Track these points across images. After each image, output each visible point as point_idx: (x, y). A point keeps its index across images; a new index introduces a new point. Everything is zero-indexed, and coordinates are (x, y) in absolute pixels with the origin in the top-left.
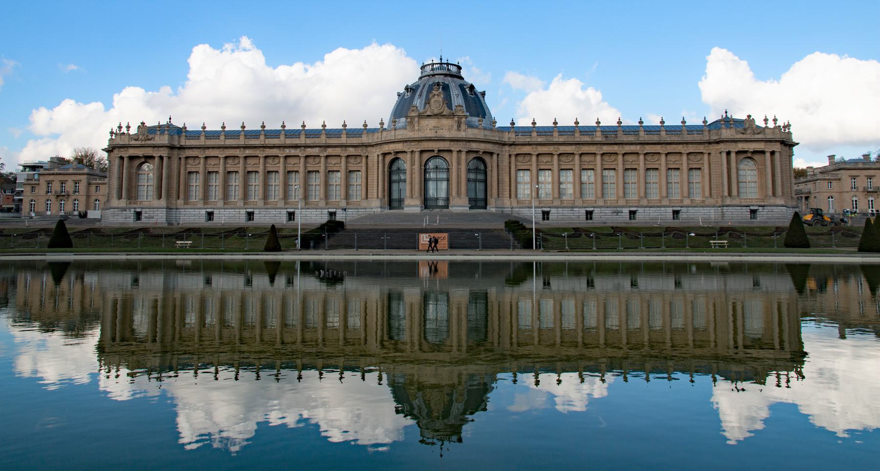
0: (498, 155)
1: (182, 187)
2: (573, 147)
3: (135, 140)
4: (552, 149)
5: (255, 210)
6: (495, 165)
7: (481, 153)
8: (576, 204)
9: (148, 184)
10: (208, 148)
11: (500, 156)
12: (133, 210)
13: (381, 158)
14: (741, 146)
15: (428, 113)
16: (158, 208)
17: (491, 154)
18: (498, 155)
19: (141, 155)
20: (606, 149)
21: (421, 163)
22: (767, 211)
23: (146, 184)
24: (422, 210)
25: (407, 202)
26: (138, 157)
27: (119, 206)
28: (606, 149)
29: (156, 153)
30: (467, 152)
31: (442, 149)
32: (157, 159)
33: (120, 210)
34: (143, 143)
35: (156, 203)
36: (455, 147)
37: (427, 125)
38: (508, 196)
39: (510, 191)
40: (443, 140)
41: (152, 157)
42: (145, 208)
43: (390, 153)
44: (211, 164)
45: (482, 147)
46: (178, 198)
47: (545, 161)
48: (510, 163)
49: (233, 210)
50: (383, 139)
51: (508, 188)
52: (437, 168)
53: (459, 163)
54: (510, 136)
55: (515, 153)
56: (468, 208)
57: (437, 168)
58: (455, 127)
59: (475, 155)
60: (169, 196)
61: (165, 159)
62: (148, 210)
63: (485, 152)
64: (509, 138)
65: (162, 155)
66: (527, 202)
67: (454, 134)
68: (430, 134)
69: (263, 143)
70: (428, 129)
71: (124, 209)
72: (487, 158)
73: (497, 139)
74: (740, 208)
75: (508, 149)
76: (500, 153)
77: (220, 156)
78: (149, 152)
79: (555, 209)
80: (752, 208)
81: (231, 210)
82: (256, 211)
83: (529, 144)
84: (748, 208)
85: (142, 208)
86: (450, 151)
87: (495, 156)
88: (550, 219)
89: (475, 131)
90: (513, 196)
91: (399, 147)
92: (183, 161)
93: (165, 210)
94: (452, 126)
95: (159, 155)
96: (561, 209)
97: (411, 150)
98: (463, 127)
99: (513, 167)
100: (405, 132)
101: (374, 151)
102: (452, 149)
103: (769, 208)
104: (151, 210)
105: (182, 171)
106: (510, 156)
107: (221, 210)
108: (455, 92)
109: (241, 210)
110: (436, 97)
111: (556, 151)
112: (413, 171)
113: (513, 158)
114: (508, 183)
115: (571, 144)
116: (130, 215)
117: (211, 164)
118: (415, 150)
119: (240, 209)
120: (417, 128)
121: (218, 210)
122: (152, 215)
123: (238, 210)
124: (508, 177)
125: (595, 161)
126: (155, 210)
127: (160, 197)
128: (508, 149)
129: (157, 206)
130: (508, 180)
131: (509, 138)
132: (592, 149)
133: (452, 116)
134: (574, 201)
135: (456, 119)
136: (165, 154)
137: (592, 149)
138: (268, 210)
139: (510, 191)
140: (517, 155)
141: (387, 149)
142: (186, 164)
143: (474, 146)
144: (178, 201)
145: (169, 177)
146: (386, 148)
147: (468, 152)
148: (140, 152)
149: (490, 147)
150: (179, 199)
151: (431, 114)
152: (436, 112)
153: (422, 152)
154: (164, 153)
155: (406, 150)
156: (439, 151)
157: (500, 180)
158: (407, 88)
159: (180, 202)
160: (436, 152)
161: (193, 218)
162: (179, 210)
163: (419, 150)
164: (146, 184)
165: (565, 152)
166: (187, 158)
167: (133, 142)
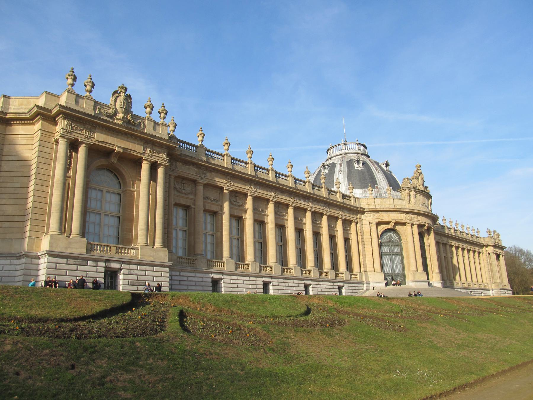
13: (374, 227)
16: (154, 265)
27: (69, 251)
32: (145, 167)
33: (72, 261)
42: (130, 263)
49: (248, 278)
62: (135, 267)
71: (83, 260)
78: (136, 148)
85: (123, 262)
91: (401, 217)
95: (154, 159)
101: (365, 218)
109: (258, 279)
123: (254, 279)
126: (148, 268)
141: (386, 218)
146: (385, 217)
155: (408, 221)
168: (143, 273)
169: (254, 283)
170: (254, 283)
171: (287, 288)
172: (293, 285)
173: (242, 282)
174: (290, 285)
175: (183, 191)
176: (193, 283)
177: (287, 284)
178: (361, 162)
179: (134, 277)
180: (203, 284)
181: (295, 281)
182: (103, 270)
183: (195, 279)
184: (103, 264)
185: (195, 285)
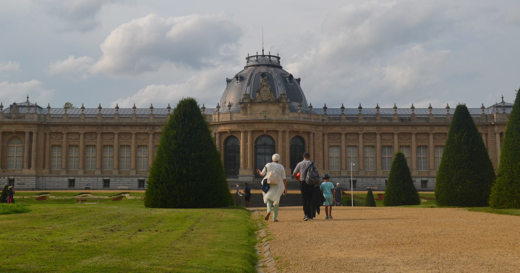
0: (314, 134)
1: (47, 159)
2: (375, 128)
3: (8, 118)
4: (357, 129)
5: (111, 178)
6: (312, 142)
7: (301, 133)
8: (378, 175)
9: (17, 155)
10: (71, 125)
11: (315, 135)
12: (7, 178)
15: (258, 100)
16: (29, 176)
17: (309, 133)
18: (314, 134)
19: (14, 131)
20: (402, 130)
21: (252, 140)
23: (15, 155)
24: (254, 179)
25: (242, 172)
26: (11, 133)
28: (402, 130)
29: (27, 130)
30: (289, 132)
31: (270, 129)
32: (27, 135)
34: (16, 120)
35: (26, 171)
36: (281, 129)
37: (258, 110)
38: (322, 167)
39: (324, 163)
40: (270, 122)
41: (24, 133)
42: (18, 176)
43: (226, 132)
44: (72, 139)
45: (302, 128)
46: (44, 167)
47: (352, 139)
48: (323, 140)
49: (92, 178)
50: (220, 121)
51: (322, 161)
52: (265, 144)
53: (284, 141)
54: (323, 118)
55: (327, 132)
57: (265, 144)
58: (281, 112)
59: (296, 134)
60: (37, 166)
61: (34, 136)
62: (20, 178)
63: (303, 132)
64: (323, 120)
65: (32, 131)
66: (337, 173)
67: (279, 117)
68: (261, 117)
69: (117, 121)
70: (258, 113)
72: (305, 137)
73: (313, 121)
75: (321, 129)
77: (80, 132)
78: (21, 128)
79: (361, 179)
81: (90, 178)
82: (112, 179)
83: (339, 126)
85: (15, 176)
86: (277, 132)
88: (357, 187)
89: (296, 115)
90: (326, 167)
91: (234, 128)
92: (48, 136)
93: (35, 178)
94: (278, 111)
95: (29, 131)
96: (366, 179)
97: (244, 130)
98: (287, 111)
99: (326, 144)
100: (239, 115)
102: (278, 129)
104: (23, 177)
105: (47, 145)
106: (323, 134)
107: (81, 178)
108: (278, 82)
109: (99, 178)
110: (265, 87)
111: (361, 131)
112: (246, 147)
113: (326, 137)
114: (322, 157)
115: (373, 126)
116: (5, 182)
117: (72, 139)
118: (247, 130)
119: (98, 177)
120: (249, 112)
121: (79, 178)
122: (24, 182)
123: (96, 178)
124: (322, 152)
125: (393, 139)
126: (26, 177)
127: (29, 167)
128: (321, 129)
129: (28, 174)
130: (322, 155)
131: (323, 120)
132: (391, 130)
133: (278, 102)
134: (376, 172)
135: (281, 105)
136: (35, 130)
137: (391, 130)
138: (122, 178)
139: (324, 163)
140: (329, 134)
143: (295, 127)
144: (44, 170)
145: (37, 149)
148: (13, 129)
149: (307, 128)
150: (44, 168)
151: (261, 101)
152: (265, 99)
153: (253, 132)
154: (34, 130)
155: (241, 130)
156: (267, 131)
157: (316, 154)
158: (237, 77)
159: (46, 171)
160: (265, 132)
161: (57, 184)
162: (45, 178)
163: (251, 130)
164: (15, 155)
165: (368, 132)
166: (51, 133)
167: (6, 120)
168: (24, 180)
169: (97, 180)
170: (97, 180)
171: (122, 182)
172: (128, 180)
173: (88, 180)
174: (125, 180)
175: (56, 138)
176: (57, 182)
177: (122, 180)
178: (239, 78)
179: (20, 182)
180: (63, 182)
181: (129, 178)
182: (7, 179)
183: (58, 180)
184: (7, 178)
185: (58, 183)
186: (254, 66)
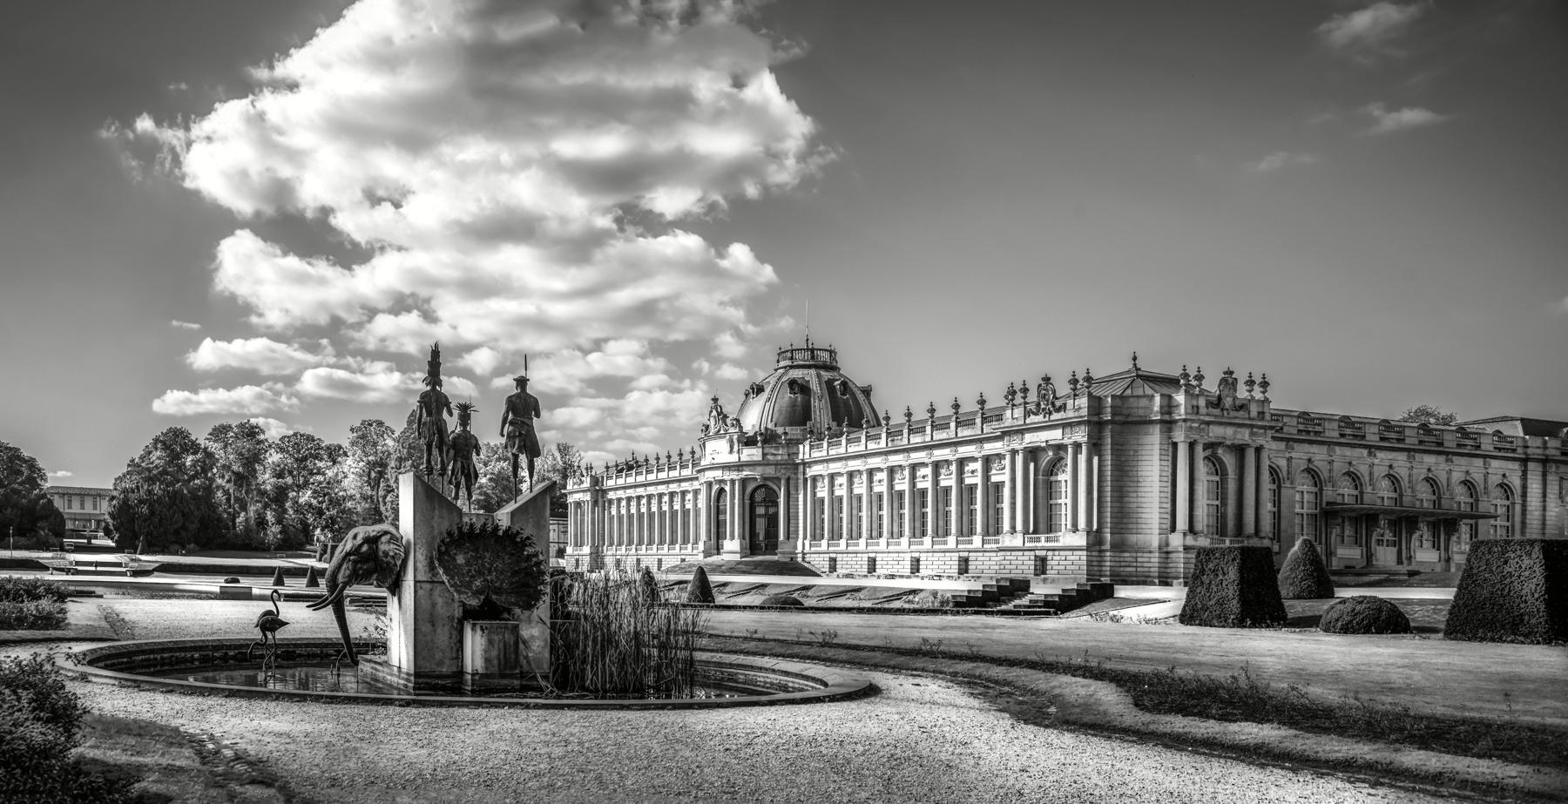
14: (1031, 439)
17: (779, 479)
22: (1058, 558)
45: (756, 473)
56: (739, 555)
74: (1021, 553)
76: (792, 476)
80: (1038, 553)
84: (1032, 553)
87: (783, 482)
102: (725, 478)
103: (1061, 553)
142: (610, 508)
143: (746, 473)
147: (744, 482)
149: (770, 471)
186: (785, 367)
